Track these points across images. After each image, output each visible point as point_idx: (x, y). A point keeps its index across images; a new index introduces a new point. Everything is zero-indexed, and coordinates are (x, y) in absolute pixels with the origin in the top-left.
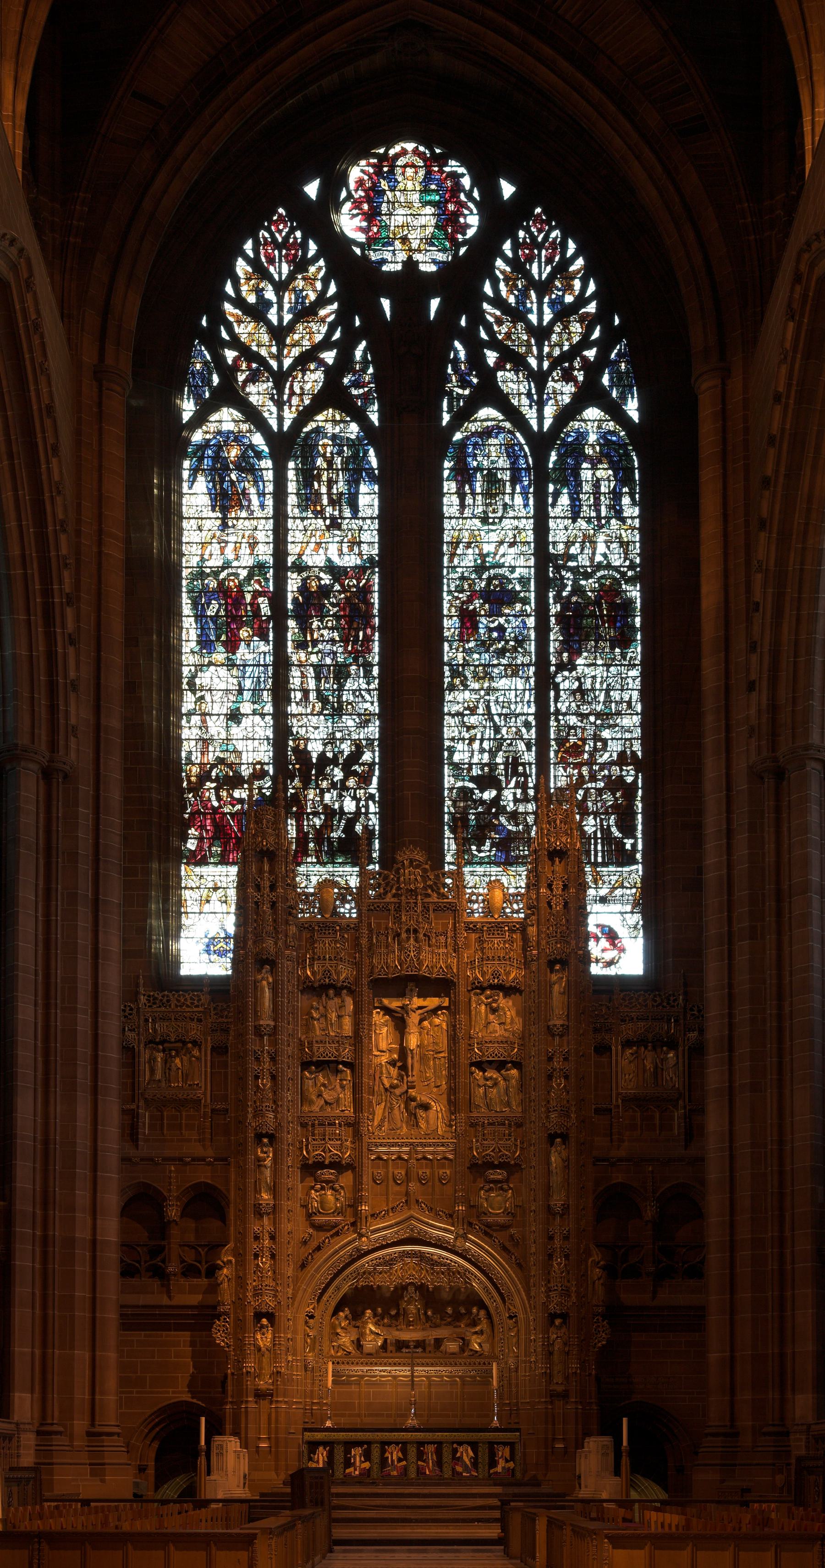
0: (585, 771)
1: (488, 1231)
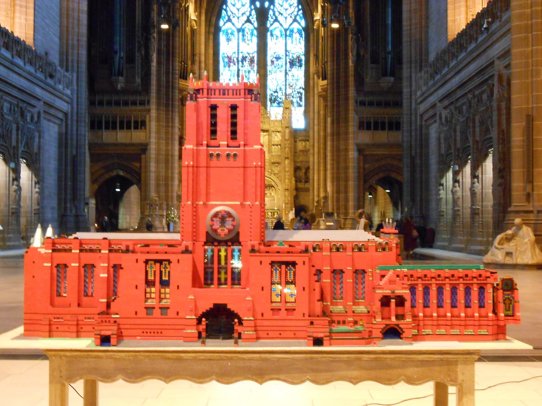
0: (293, 90)
1: (275, 174)
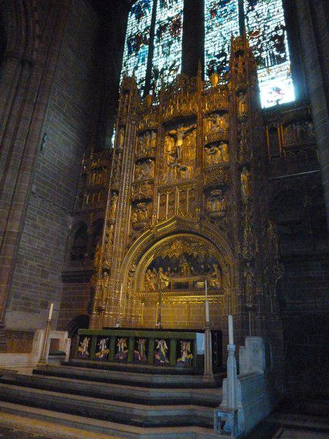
0: (261, 38)
